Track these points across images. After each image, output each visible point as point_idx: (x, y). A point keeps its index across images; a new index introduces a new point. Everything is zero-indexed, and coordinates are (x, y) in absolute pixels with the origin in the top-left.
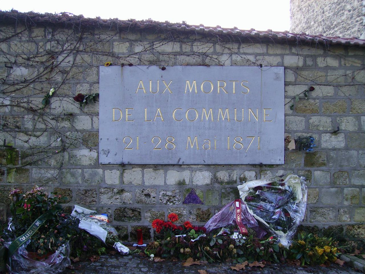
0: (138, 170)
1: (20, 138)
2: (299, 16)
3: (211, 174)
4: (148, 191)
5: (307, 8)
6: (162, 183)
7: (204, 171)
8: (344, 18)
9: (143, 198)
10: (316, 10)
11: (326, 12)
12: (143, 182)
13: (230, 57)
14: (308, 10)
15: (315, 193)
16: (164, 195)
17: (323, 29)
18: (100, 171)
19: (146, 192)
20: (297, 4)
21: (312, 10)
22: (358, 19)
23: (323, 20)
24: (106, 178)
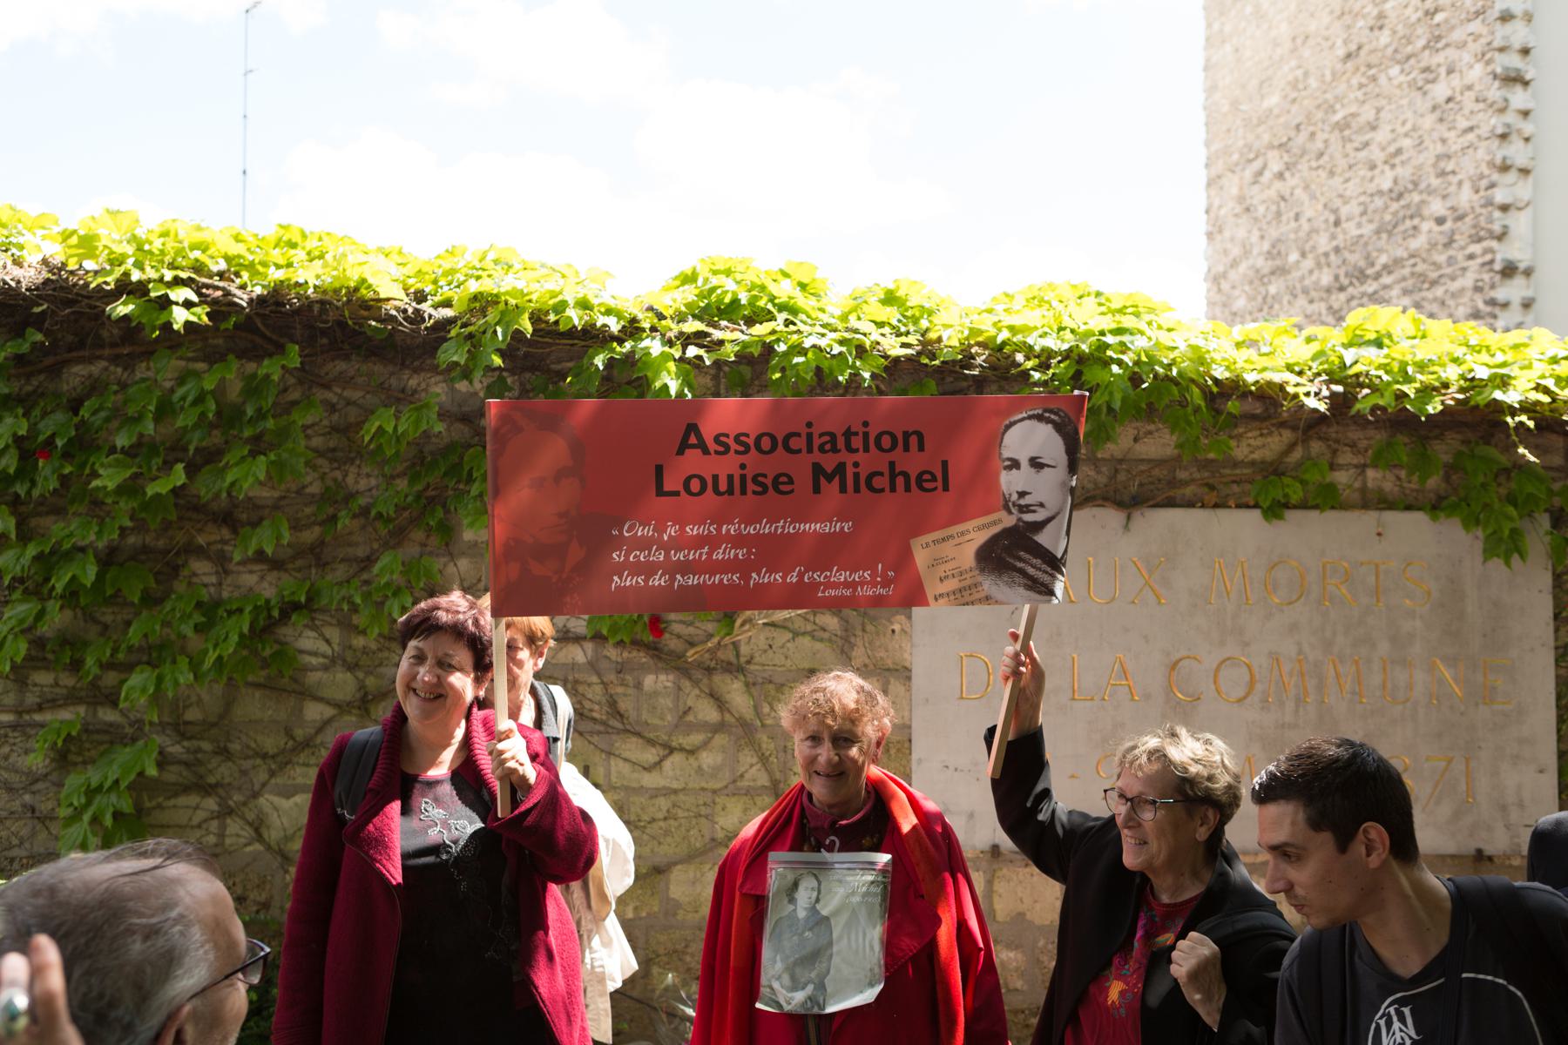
1: (626, 754)
2: (1241, 233)
5: (1274, 208)
8: (1418, 243)
10: (1309, 213)
11: (1348, 220)
13: (1360, 478)
14: (1279, 214)
17: (1337, 278)
20: (1235, 191)
21: (1292, 214)
22: (1476, 248)
23: (1337, 250)
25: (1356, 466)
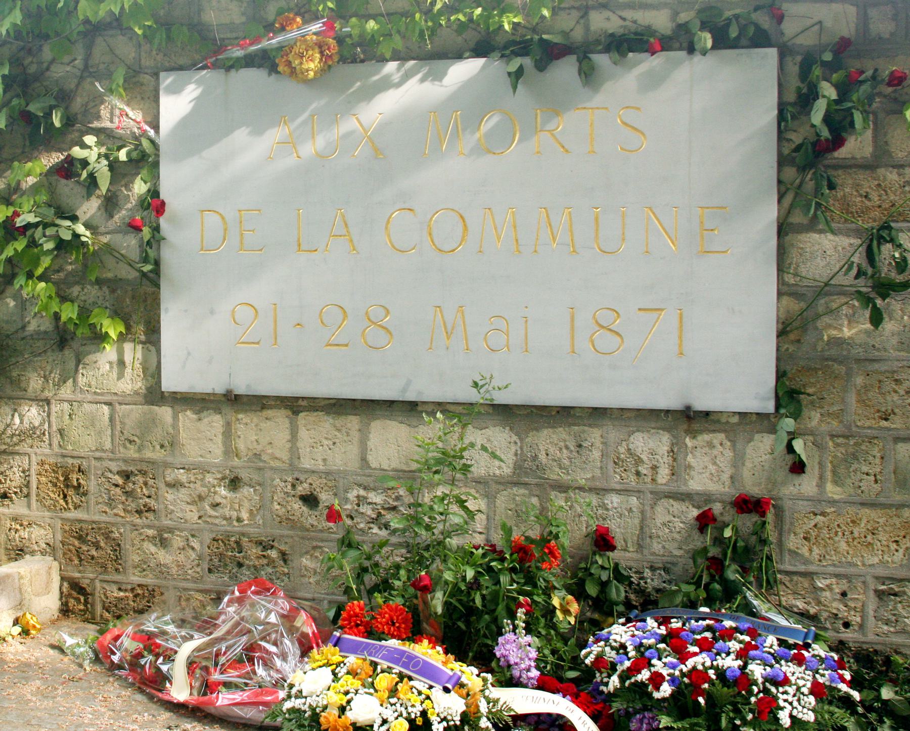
0: (280, 419)
3: (515, 438)
4: (311, 484)
6: (354, 464)
7: (492, 428)
9: (297, 506)
12: (294, 452)
13: (582, 21)
15: (899, 526)
16: (360, 500)
18: (165, 413)
19: (302, 489)
24: (183, 434)
25: (578, 9)
